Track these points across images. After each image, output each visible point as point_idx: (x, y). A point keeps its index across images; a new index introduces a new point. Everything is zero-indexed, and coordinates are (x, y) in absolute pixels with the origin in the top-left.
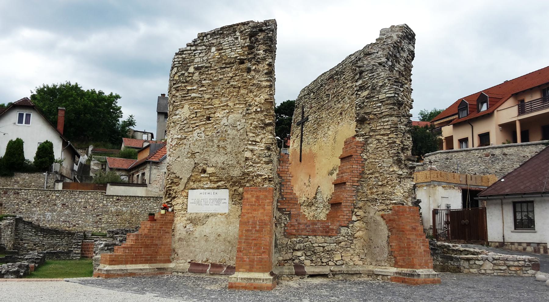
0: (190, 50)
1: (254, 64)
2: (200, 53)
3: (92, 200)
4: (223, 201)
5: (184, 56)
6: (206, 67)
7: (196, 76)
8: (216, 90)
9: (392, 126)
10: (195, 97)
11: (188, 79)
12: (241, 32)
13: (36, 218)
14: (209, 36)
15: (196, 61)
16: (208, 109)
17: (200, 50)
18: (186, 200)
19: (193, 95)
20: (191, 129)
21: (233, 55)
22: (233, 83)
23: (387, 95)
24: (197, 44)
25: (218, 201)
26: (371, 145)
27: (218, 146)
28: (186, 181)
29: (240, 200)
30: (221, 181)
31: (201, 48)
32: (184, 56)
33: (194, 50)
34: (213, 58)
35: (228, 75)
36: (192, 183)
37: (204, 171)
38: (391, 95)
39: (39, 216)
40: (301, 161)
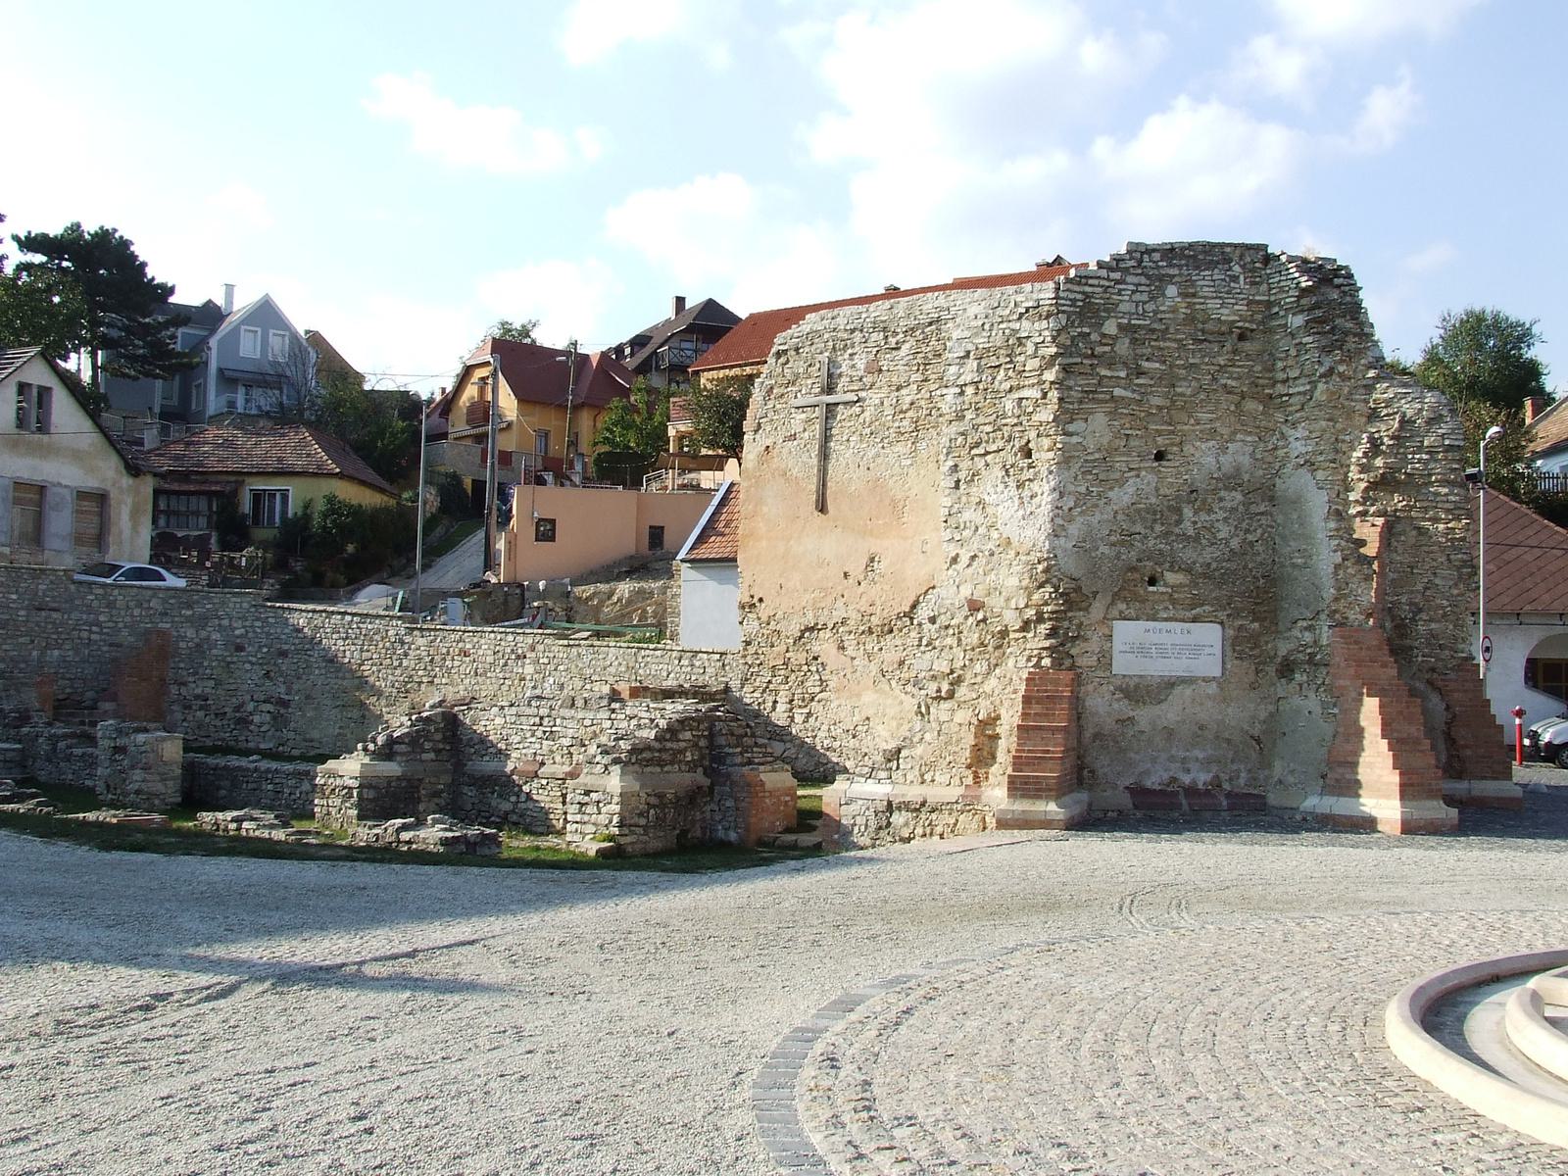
0: (1108, 279)
1: (1341, 361)
2: (1133, 292)
4: (1207, 650)
5: (1088, 289)
6: (1153, 331)
7: (1123, 347)
8: (1179, 390)
9: (1462, 505)
10: (1123, 398)
11: (1099, 350)
12: (1243, 267)
14: (1156, 256)
15: (1123, 307)
16: (1159, 433)
17: (1137, 285)
18: (1109, 645)
19: (1117, 392)
20: (1117, 475)
21: (1226, 315)
22: (1229, 382)
23: (1447, 442)
24: (1127, 269)
25: (1196, 650)
26: (1403, 538)
27: (1195, 523)
28: (1109, 599)
29: (1251, 649)
30: (1202, 605)
31: (1136, 280)
32: (1088, 289)
33: (1118, 282)
34: (1173, 312)
35: (1215, 361)
36: (1124, 606)
37: (1152, 582)
38: (1457, 443)
40: (822, 507)
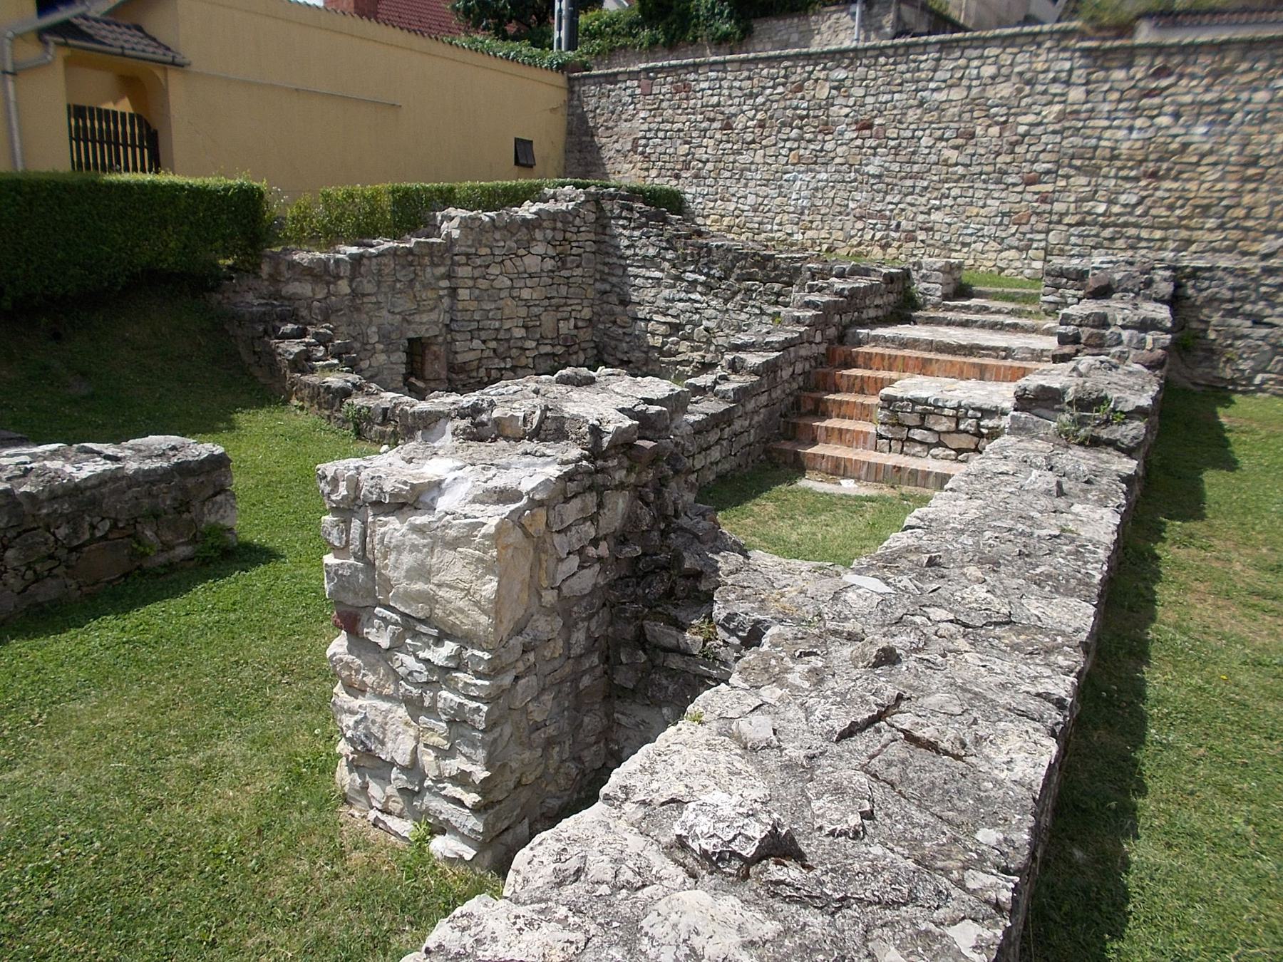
3: (1005, 90)
13: (751, 199)
39: (763, 191)
